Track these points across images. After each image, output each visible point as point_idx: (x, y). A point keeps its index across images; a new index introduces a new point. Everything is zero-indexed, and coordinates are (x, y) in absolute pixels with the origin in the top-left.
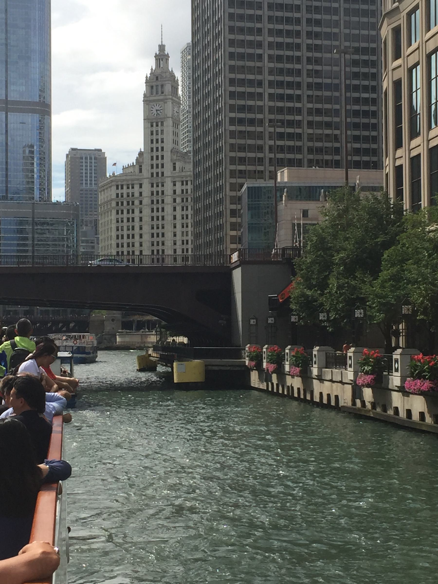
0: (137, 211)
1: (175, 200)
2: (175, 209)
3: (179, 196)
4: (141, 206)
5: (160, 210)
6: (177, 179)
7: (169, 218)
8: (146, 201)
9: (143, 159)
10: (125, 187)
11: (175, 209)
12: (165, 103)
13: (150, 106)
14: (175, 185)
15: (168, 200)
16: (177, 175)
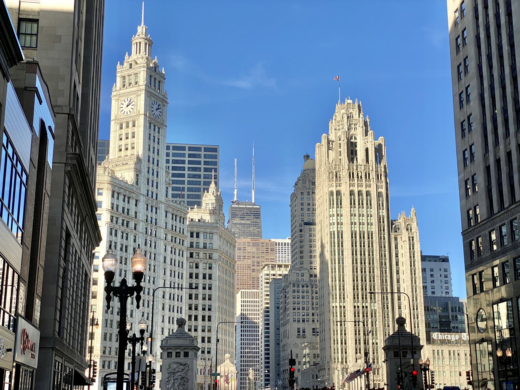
0: (131, 238)
5: (153, 244)
8: (141, 227)
10: (121, 197)
14: (166, 217)
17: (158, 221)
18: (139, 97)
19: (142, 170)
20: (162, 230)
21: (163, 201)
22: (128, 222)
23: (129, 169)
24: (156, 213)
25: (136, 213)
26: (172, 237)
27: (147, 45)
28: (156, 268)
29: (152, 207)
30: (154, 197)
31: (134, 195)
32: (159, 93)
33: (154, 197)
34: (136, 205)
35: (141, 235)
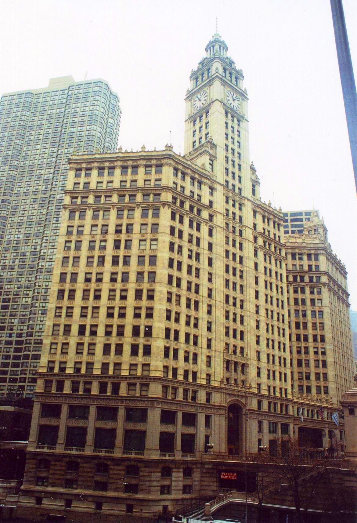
0: (205, 229)
1: (255, 238)
2: (256, 255)
3: (260, 233)
4: (210, 224)
5: (238, 245)
6: (258, 209)
7: (249, 263)
8: (219, 220)
9: (215, 153)
10: (188, 179)
11: (256, 255)
12: (243, 100)
13: (226, 91)
14: (255, 216)
15: (248, 234)
16: (257, 202)
17: (243, 219)
18: (212, 87)
19: (218, 157)
20: (251, 231)
21: (250, 198)
22: (199, 211)
23: (201, 154)
24: (240, 209)
25: (211, 202)
26: (265, 242)
27: (222, 48)
28: (244, 274)
29: (234, 201)
30: (237, 191)
31: (207, 181)
32: (237, 86)
33: (237, 191)
34: (211, 194)
35: (219, 229)
